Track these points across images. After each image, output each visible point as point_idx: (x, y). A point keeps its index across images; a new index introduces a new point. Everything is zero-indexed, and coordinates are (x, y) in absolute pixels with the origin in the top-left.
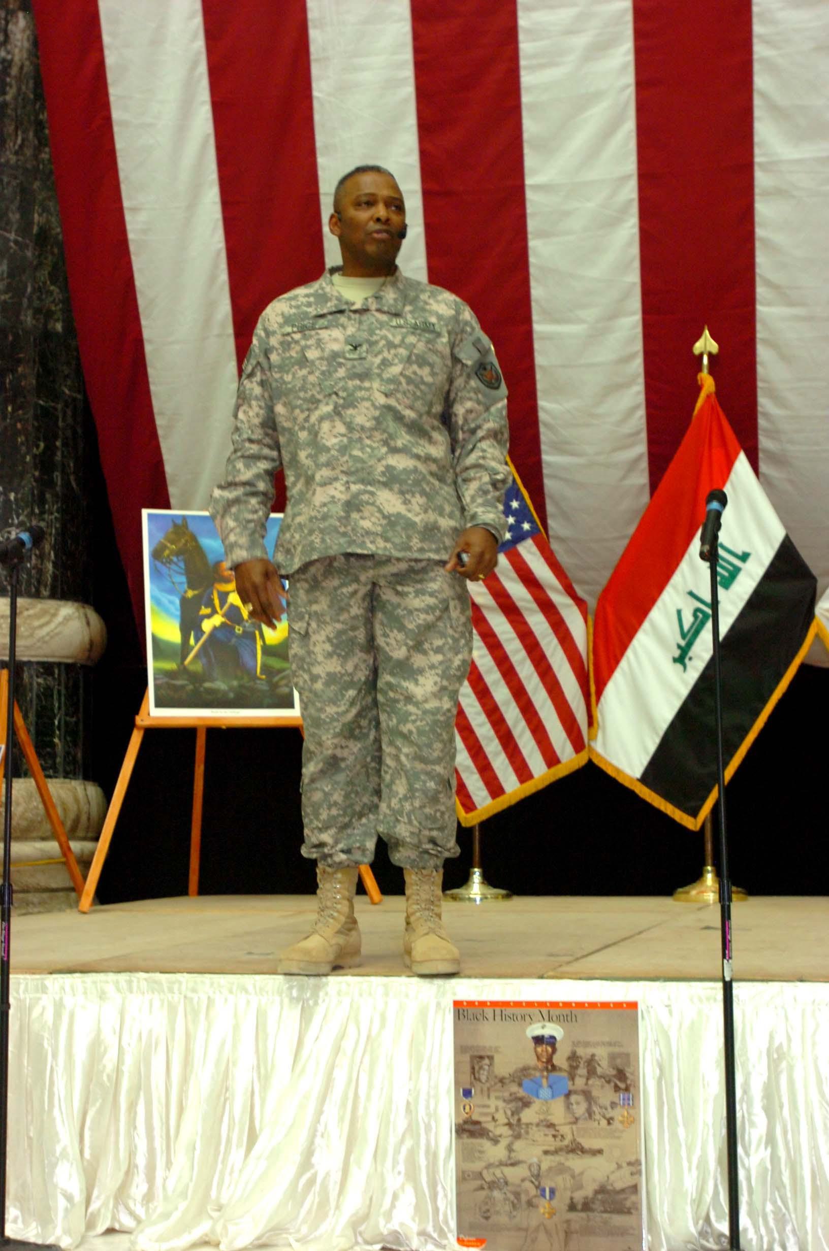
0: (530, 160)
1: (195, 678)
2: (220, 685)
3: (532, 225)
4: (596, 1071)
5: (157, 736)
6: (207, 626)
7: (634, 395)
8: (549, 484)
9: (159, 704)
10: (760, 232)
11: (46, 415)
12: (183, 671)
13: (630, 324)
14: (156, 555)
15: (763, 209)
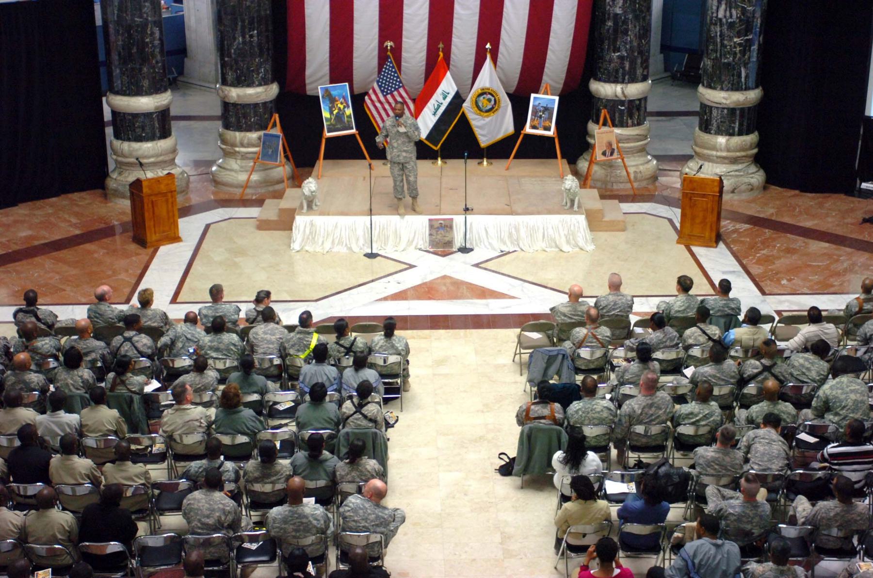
0: (405, 7)
1: (334, 125)
2: (339, 126)
3: (404, 20)
4: (448, 226)
5: (329, 140)
6: (335, 113)
7: (423, 55)
8: (403, 68)
9: (329, 132)
10: (454, 25)
11: (267, 36)
12: (331, 124)
13: (424, 41)
14: (323, 97)
15: (455, 21)
